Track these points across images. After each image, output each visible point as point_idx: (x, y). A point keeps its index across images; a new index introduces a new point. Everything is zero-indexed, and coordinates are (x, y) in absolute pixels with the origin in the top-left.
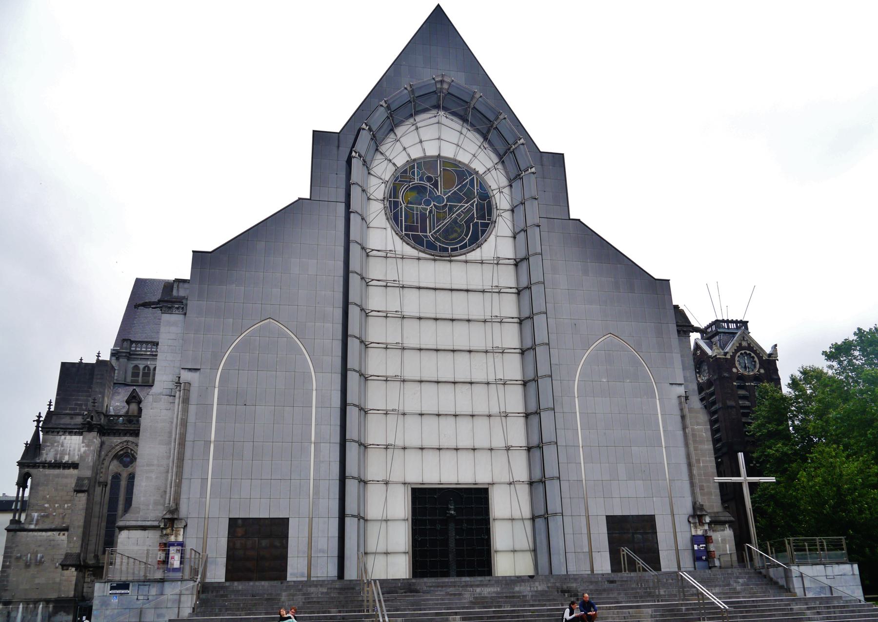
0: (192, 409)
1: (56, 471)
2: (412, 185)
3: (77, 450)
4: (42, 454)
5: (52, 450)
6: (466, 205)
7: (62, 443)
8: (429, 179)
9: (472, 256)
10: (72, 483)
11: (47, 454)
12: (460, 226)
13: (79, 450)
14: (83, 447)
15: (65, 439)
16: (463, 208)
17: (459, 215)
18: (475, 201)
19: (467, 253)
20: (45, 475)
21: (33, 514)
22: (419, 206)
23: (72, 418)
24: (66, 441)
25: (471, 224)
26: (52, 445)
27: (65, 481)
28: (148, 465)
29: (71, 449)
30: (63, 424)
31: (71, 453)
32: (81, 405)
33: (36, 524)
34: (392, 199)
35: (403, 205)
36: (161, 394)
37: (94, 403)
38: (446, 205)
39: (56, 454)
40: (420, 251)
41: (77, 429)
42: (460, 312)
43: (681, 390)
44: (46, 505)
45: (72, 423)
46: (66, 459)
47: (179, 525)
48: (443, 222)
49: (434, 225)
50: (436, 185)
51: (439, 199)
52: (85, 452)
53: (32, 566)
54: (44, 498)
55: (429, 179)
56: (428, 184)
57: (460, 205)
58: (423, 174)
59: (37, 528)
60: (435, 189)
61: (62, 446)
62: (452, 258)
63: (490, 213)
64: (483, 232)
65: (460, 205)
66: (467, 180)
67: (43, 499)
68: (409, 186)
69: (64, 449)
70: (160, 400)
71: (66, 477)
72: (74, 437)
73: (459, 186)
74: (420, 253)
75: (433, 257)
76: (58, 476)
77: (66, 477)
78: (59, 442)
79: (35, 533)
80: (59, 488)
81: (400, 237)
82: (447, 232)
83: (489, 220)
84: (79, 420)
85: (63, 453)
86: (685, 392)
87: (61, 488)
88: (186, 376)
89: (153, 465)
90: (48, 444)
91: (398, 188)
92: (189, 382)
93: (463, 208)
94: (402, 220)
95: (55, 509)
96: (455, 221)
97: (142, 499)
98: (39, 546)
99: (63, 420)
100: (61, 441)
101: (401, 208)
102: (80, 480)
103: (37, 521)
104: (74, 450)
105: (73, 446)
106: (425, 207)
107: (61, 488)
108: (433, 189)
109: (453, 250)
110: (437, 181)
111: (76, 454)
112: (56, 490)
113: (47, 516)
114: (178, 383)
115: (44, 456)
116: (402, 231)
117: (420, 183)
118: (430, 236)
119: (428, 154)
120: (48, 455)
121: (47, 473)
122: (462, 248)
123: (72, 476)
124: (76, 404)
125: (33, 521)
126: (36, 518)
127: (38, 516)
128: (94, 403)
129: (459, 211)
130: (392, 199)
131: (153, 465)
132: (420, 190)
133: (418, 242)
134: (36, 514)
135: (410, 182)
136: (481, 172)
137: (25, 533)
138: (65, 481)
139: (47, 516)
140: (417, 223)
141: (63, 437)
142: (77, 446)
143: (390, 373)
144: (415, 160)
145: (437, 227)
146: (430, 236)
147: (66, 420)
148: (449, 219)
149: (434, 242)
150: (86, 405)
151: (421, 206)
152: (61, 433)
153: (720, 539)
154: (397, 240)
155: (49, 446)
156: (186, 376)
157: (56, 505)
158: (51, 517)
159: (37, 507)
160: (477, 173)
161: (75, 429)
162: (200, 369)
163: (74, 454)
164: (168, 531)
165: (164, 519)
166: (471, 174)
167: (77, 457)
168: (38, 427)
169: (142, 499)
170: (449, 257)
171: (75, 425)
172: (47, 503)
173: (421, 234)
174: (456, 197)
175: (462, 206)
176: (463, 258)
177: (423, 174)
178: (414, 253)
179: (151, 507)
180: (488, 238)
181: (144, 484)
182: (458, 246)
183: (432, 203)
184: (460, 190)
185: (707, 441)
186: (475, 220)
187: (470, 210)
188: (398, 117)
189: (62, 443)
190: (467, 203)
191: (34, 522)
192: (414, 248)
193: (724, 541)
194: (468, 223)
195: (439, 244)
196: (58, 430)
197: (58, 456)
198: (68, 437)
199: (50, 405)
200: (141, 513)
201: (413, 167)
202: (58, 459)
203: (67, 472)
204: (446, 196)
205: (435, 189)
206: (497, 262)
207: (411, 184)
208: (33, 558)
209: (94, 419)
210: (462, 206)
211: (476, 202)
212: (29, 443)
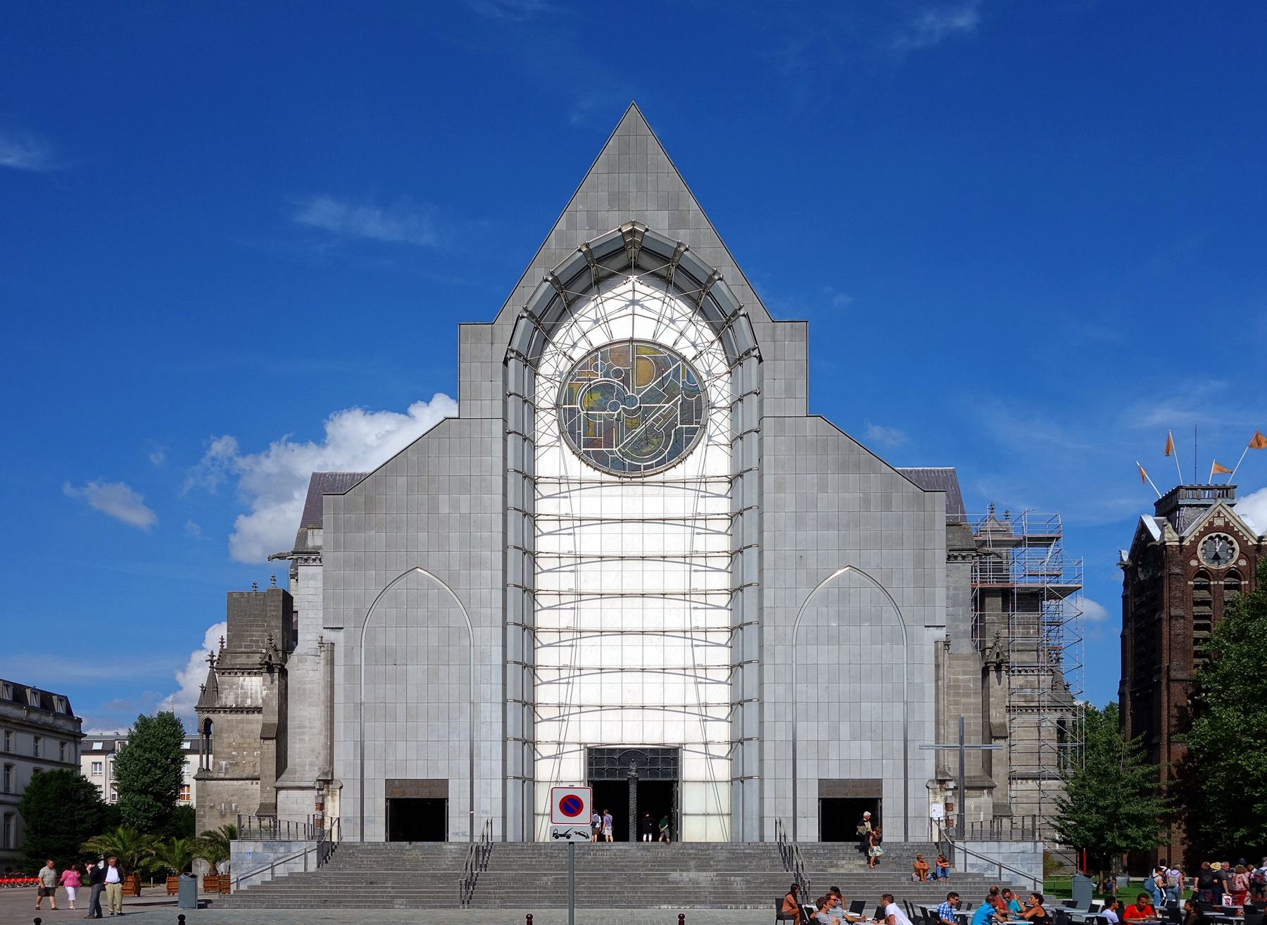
0: (339, 671)
1: (240, 716)
2: (594, 383)
3: (259, 692)
4: (221, 698)
5: (232, 693)
6: (667, 406)
7: (242, 684)
8: (617, 374)
9: (671, 474)
10: (258, 729)
11: (226, 698)
12: (657, 436)
13: (262, 693)
14: (265, 690)
15: (244, 680)
16: (663, 410)
17: (657, 420)
18: (679, 399)
19: (665, 470)
20: (228, 721)
21: (221, 762)
22: (603, 413)
23: (248, 657)
24: (245, 683)
25: (673, 432)
26: (231, 687)
27: (250, 727)
28: (299, 727)
29: (253, 691)
30: (239, 664)
31: (254, 696)
32: (257, 641)
33: (226, 773)
34: (567, 406)
35: (582, 413)
36: (307, 654)
37: (271, 640)
38: (640, 407)
39: (237, 698)
40: (603, 472)
41: (257, 669)
42: (652, 548)
43: (941, 634)
44: (234, 753)
45: (250, 663)
46: (249, 703)
47: (335, 785)
48: (632, 433)
49: (622, 437)
50: (625, 381)
51: (632, 400)
52: (267, 695)
53: (228, 815)
54: (230, 745)
55: (617, 374)
56: (616, 380)
57: (659, 405)
58: (610, 367)
59: (227, 777)
60: (625, 387)
61: (242, 689)
62: (646, 479)
63: (699, 416)
64: (689, 440)
65: (659, 405)
66: (669, 371)
67: (229, 747)
68: (590, 385)
69: (244, 692)
70: (306, 661)
71: (249, 722)
72: (254, 678)
73: (658, 380)
74: (603, 474)
75: (616, 479)
76: (242, 721)
77: (249, 722)
78: (238, 684)
79: (226, 782)
80: (245, 735)
81: (577, 455)
82: (639, 446)
83: (698, 423)
84: (257, 659)
85: (245, 696)
86: (947, 635)
87: (248, 734)
88: (330, 636)
89: (305, 727)
90: (226, 687)
91: (575, 389)
92: (332, 642)
93: (663, 410)
94: (579, 434)
95: (244, 758)
96: (650, 430)
97: (297, 760)
98: (232, 796)
99: (239, 659)
100: (240, 684)
101: (580, 417)
102: (265, 726)
103: (226, 769)
104: (256, 693)
105: (254, 688)
106: (611, 413)
107: (248, 734)
108: (624, 389)
109: (646, 468)
110: (627, 374)
111: (259, 697)
112: (242, 737)
113: (236, 764)
114: (321, 644)
115: (224, 700)
116: (580, 447)
117: (607, 381)
118: (618, 453)
119: (617, 337)
120: (229, 699)
121: (229, 718)
122: (658, 464)
123: (257, 721)
124: (251, 641)
125: (221, 770)
126: (224, 766)
127: (226, 765)
128: (271, 640)
129: (657, 415)
130: (567, 406)
131: (305, 727)
132: (606, 389)
133: (600, 461)
134: (224, 763)
135: (590, 380)
136: (689, 357)
137: (216, 782)
138: (250, 727)
139: (236, 764)
140: (600, 436)
141: (241, 678)
142: (259, 689)
143: (563, 625)
144: (598, 349)
145: (626, 438)
146: (618, 453)
147: (242, 660)
148: (644, 426)
149: (623, 459)
150: (263, 642)
151: (606, 412)
152: (239, 674)
153: (973, 807)
154: (573, 461)
155: (227, 689)
156: (330, 636)
157: (245, 753)
158: (241, 765)
159: (223, 755)
160: (684, 359)
161: (254, 669)
162: (342, 628)
163: (257, 697)
164: (325, 792)
165: (319, 780)
166: (675, 361)
167: (261, 700)
168: (212, 667)
169: (297, 760)
170: (641, 477)
171: (253, 664)
172: (235, 751)
173: (604, 449)
174: (653, 396)
175: (660, 408)
176: (660, 477)
177: (610, 367)
178: (597, 475)
179: (307, 768)
180: (693, 449)
181: (297, 746)
182: (654, 462)
183: (621, 406)
184: (661, 384)
185: (975, 693)
186: (679, 426)
187: (671, 410)
188: (547, 323)
189: (242, 684)
190: (667, 402)
191: (224, 771)
192: (595, 469)
193: (978, 808)
194: (668, 430)
195: (628, 461)
196: (235, 671)
197: (240, 700)
198: (248, 679)
199: (222, 643)
200: (298, 775)
201: (596, 358)
202: (239, 703)
203: (251, 716)
204: (640, 396)
205: (625, 387)
206: (703, 479)
207: (592, 382)
208: (227, 807)
209: (273, 658)
210: (660, 408)
211: (680, 402)
212: (204, 685)
